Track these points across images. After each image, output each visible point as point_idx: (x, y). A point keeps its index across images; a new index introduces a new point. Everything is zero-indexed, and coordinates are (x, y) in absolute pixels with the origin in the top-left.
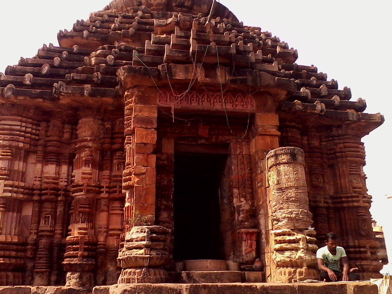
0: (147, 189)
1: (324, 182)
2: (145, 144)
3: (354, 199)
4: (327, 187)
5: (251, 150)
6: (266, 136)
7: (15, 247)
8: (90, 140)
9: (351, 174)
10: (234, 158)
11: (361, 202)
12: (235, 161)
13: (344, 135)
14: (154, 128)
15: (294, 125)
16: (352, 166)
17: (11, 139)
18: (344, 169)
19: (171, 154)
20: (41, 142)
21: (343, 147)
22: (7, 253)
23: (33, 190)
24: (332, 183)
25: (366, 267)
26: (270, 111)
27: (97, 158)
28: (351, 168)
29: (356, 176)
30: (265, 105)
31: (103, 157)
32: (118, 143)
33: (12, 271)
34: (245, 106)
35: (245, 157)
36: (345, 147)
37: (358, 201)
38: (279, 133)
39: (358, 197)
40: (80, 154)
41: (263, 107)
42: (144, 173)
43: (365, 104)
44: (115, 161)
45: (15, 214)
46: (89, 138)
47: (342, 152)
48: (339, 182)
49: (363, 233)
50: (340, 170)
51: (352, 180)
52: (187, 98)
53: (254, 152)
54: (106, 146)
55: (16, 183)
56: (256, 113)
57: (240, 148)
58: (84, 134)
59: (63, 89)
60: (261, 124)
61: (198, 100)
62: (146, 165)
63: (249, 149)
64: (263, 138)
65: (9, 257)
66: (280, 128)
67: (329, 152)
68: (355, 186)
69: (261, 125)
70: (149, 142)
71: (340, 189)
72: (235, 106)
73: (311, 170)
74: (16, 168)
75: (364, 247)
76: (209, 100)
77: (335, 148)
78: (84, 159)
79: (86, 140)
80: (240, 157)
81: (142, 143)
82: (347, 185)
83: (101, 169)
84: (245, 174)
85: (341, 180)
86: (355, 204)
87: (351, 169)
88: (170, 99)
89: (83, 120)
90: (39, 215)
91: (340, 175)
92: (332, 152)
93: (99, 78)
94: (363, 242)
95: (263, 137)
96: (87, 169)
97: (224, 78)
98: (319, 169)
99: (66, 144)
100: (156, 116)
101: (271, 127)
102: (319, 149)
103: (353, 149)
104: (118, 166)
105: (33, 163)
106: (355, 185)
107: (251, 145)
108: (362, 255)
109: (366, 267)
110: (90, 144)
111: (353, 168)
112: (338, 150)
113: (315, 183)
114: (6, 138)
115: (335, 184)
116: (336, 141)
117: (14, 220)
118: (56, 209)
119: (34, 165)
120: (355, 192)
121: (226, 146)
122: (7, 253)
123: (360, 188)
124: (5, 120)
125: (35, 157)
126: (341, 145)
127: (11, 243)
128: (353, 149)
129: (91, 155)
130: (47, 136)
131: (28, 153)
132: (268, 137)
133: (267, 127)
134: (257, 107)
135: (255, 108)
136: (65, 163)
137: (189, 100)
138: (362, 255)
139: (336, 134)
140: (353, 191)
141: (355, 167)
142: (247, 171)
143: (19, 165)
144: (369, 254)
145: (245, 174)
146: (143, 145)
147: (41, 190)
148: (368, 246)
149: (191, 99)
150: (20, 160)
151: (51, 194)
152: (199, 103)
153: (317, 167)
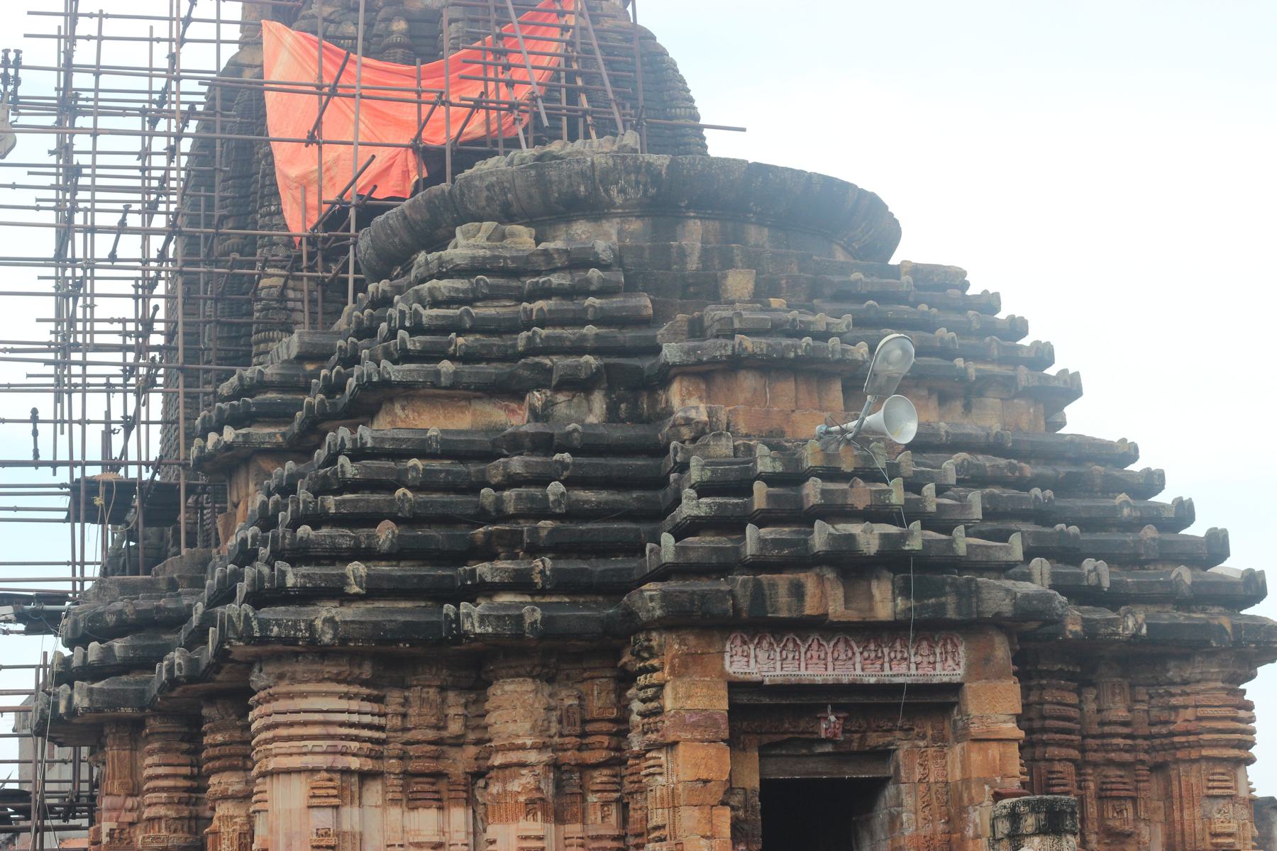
1: (1137, 818)
2: (706, 782)
4: (1145, 831)
5: (949, 770)
6: (991, 743)
8: (533, 747)
9: (1209, 797)
10: (909, 793)
12: (908, 801)
13: (1198, 681)
14: (723, 741)
15: (1061, 670)
16: (1213, 774)
17: (330, 750)
18: (1193, 780)
20: (394, 748)
21: (1192, 718)
24: (1163, 818)
26: (999, 676)
27: (548, 789)
28: (1211, 778)
29: (1222, 802)
30: (987, 660)
31: (559, 785)
32: (601, 748)
34: (938, 666)
35: (934, 788)
36: (1199, 719)
38: (1022, 734)
40: (505, 781)
41: (980, 667)
43: (1264, 583)
44: (592, 798)
46: (529, 742)
47: (1188, 733)
48: (1177, 815)
50: (1183, 784)
51: (1211, 812)
52: (797, 654)
53: (958, 778)
54: (570, 756)
56: (967, 685)
57: (922, 765)
58: (511, 727)
59: (473, 625)
60: (977, 714)
61: (822, 656)
62: (708, 834)
63: (944, 767)
64: (980, 749)
66: (1019, 719)
67: (1155, 730)
68: (1218, 830)
69: (977, 717)
70: (712, 776)
71: (1178, 838)
72: (913, 666)
73: (1104, 787)
74: (346, 827)
76: (850, 654)
77: (1173, 718)
78: (522, 799)
79: (522, 748)
80: (922, 787)
81: (698, 780)
82: (1199, 826)
83: (559, 818)
84: (934, 833)
85: (1182, 811)
87: (1209, 780)
88: (756, 657)
89: (508, 688)
91: (1181, 797)
92: (1164, 731)
93: (548, 573)
95: (982, 745)
96: (534, 826)
97: (890, 605)
98: (1124, 783)
99: (451, 745)
100: (727, 708)
101: (1002, 718)
102: (1125, 724)
104: (603, 811)
105: (376, 807)
106: (1218, 828)
107: (949, 758)
110: (532, 757)
111: (1216, 777)
112: (1180, 725)
113: (1110, 823)
114: (317, 749)
115: (1169, 822)
116: (1174, 701)
119: (379, 811)
121: (885, 754)
123: (1230, 835)
124: (304, 695)
125: (380, 788)
126: (1189, 713)
128: (1220, 725)
129: (538, 789)
130: (405, 730)
132: (994, 744)
133: (994, 719)
134: (969, 667)
135: (961, 671)
136: (456, 801)
137: (803, 659)
139: (1178, 680)
140: (1212, 844)
141: (1223, 774)
142: (941, 827)
145: (934, 833)
146: (700, 785)
149: (806, 653)
152: (826, 665)
153: (1121, 777)
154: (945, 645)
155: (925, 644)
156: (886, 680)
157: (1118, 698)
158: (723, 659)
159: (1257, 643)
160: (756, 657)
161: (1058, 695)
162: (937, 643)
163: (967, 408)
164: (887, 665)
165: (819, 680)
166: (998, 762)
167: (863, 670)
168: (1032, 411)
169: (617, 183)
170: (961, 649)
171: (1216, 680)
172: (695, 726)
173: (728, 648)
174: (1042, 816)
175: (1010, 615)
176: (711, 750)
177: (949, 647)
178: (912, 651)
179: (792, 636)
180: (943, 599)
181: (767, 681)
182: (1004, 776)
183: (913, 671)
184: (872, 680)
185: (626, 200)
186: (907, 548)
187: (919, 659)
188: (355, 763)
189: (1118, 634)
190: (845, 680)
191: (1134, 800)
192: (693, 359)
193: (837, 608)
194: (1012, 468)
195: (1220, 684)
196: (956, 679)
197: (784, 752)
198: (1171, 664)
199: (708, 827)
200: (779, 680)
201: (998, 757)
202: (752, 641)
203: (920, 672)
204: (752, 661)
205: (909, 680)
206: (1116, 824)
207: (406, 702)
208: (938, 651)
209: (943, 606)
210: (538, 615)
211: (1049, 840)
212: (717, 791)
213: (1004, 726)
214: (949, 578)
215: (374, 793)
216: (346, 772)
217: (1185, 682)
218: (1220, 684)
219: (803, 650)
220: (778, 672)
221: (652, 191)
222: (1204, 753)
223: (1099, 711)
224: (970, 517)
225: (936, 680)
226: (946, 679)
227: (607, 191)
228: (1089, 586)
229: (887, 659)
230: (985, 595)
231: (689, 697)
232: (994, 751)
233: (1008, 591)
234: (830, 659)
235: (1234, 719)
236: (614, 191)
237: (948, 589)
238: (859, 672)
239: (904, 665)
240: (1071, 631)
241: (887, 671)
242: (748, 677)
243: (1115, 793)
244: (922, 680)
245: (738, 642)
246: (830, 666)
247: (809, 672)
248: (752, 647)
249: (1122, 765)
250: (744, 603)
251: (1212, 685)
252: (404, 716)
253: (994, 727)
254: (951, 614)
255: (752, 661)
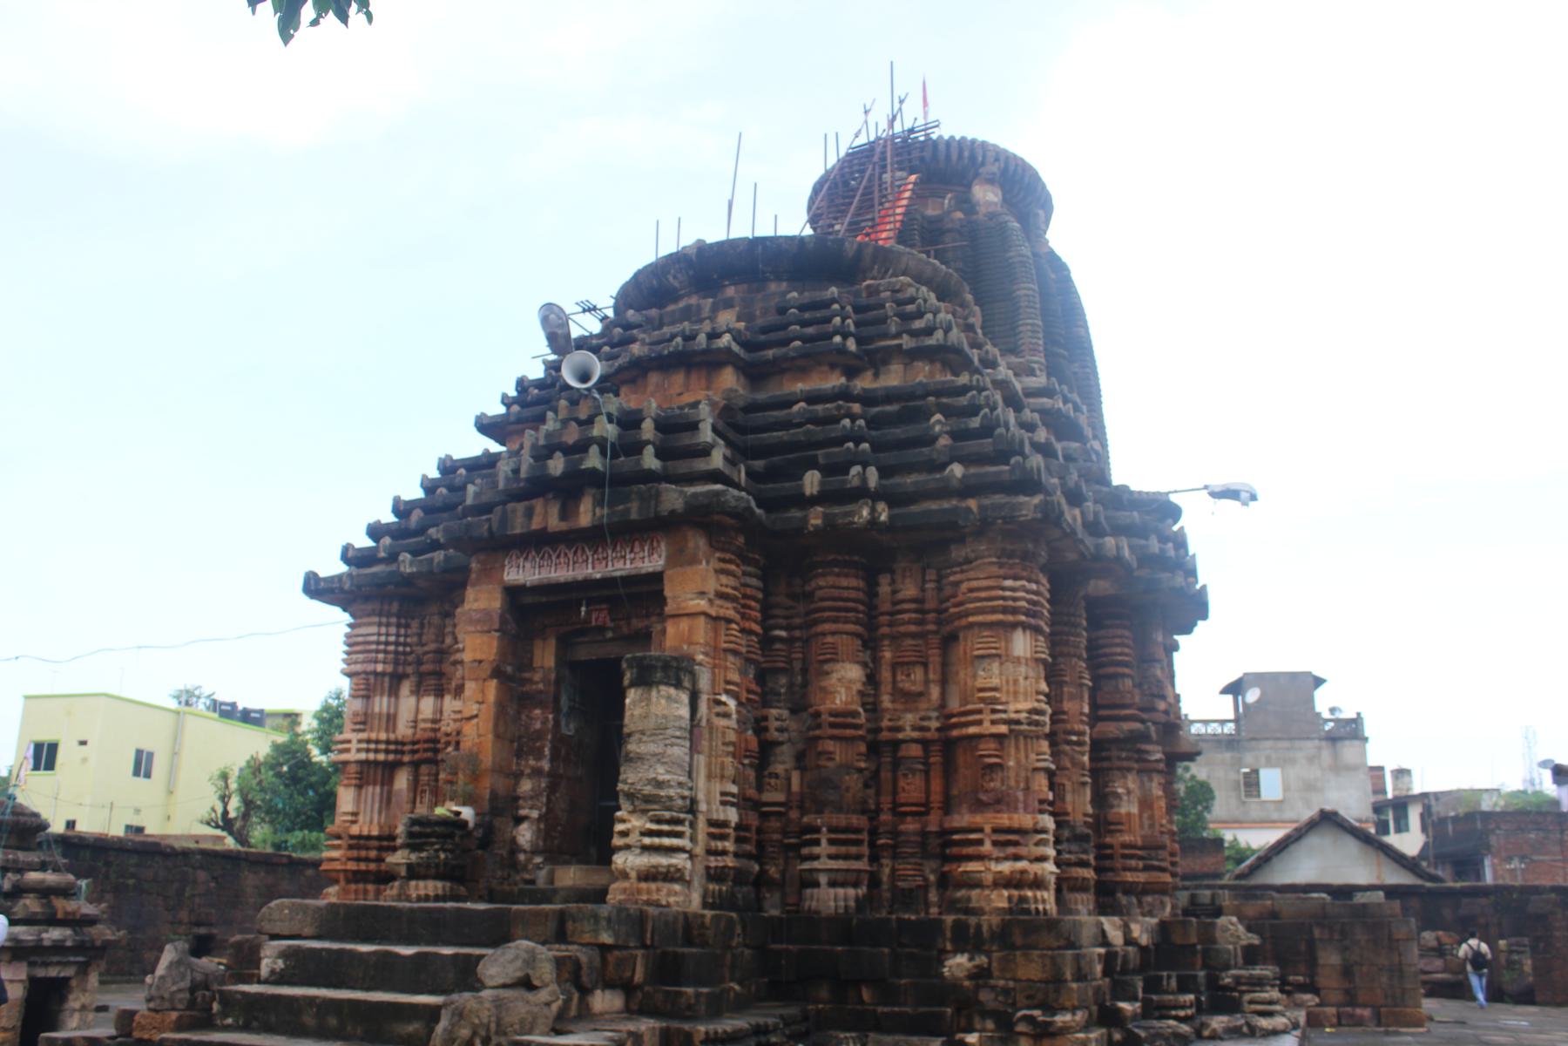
0: (480, 743)
1: (927, 682)
2: (480, 662)
3: (971, 718)
7: (375, 843)
11: (987, 724)
19: (550, 669)
22: (363, 853)
23: (403, 744)
25: (978, 875)
33: (374, 882)
34: (646, 560)
37: (979, 723)
39: (980, 712)
41: (679, 558)
42: (476, 716)
45: (378, 789)
49: (984, 797)
55: (373, 736)
65: (367, 860)
70: (483, 657)
72: (628, 562)
75: (981, 830)
81: (475, 661)
86: (972, 730)
90: (415, 785)
94: (978, 819)
95: (676, 620)
98: (919, 651)
101: (690, 596)
103: (983, 594)
106: (980, 683)
108: (970, 850)
109: (978, 875)
113: (901, 685)
117: (377, 799)
118: (437, 774)
120: (982, 700)
122: (363, 853)
127: (369, 838)
128: (983, 594)
131: (397, 679)
135: (661, 562)
138: (970, 850)
141: (992, 637)
143: (381, 704)
144: (987, 847)
146: (476, 664)
147: (414, 743)
148: (988, 829)
150: (382, 695)
151: (426, 750)
154: (652, 541)
155: (637, 543)
156: (608, 575)
157: (908, 581)
158: (503, 571)
159: (1003, 518)
160: (524, 567)
161: (831, 580)
162: (646, 541)
163: (876, 375)
164: (610, 564)
165: (562, 580)
166: (686, 633)
167: (593, 568)
168: (927, 368)
169: (669, 273)
170: (663, 546)
171: (990, 556)
172: (478, 621)
173: (506, 562)
174: (635, 670)
175: (680, 511)
176: (485, 638)
177: (655, 544)
178: (628, 550)
179: (547, 548)
180: (629, 505)
181: (528, 584)
182: (690, 643)
183: (628, 566)
184: (598, 576)
185: (681, 282)
186: (583, 467)
187: (632, 555)
188: (380, 668)
189: (855, 523)
190: (580, 578)
191: (925, 665)
192: (613, 370)
193: (554, 523)
194: (839, 408)
195: (994, 560)
196: (659, 569)
197: (586, 639)
198: (953, 547)
199: (481, 695)
200: (536, 583)
201: (687, 628)
202: (522, 554)
203: (633, 566)
204: (521, 571)
205: (623, 573)
206: (907, 686)
207: (422, 626)
208: (646, 548)
209: (628, 511)
210: (442, 557)
211: (640, 691)
212: (487, 669)
213: (691, 603)
214: (635, 488)
215: (406, 688)
216: (375, 673)
217: (968, 561)
218: (994, 560)
219: (554, 558)
220: (537, 577)
221: (691, 273)
222: (971, 619)
223: (894, 592)
224: (698, 441)
225: (643, 571)
226: (651, 570)
227: (667, 279)
228: (852, 489)
229: (610, 558)
230: (664, 497)
231: (476, 600)
232: (684, 624)
233: (681, 492)
234: (571, 562)
235: (1004, 589)
236: (670, 278)
237: (633, 496)
238: (590, 570)
239: (622, 562)
240: (812, 525)
241: (610, 568)
242: (516, 583)
243: (906, 659)
244: (634, 572)
245: (514, 557)
246: (571, 568)
247: (557, 574)
248: (522, 560)
249: (913, 636)
250: (495, 526)
251: (986, 560)
252: (420, 635)
253: (683, 605)
254: (634, 516)
255: (521, 571)
